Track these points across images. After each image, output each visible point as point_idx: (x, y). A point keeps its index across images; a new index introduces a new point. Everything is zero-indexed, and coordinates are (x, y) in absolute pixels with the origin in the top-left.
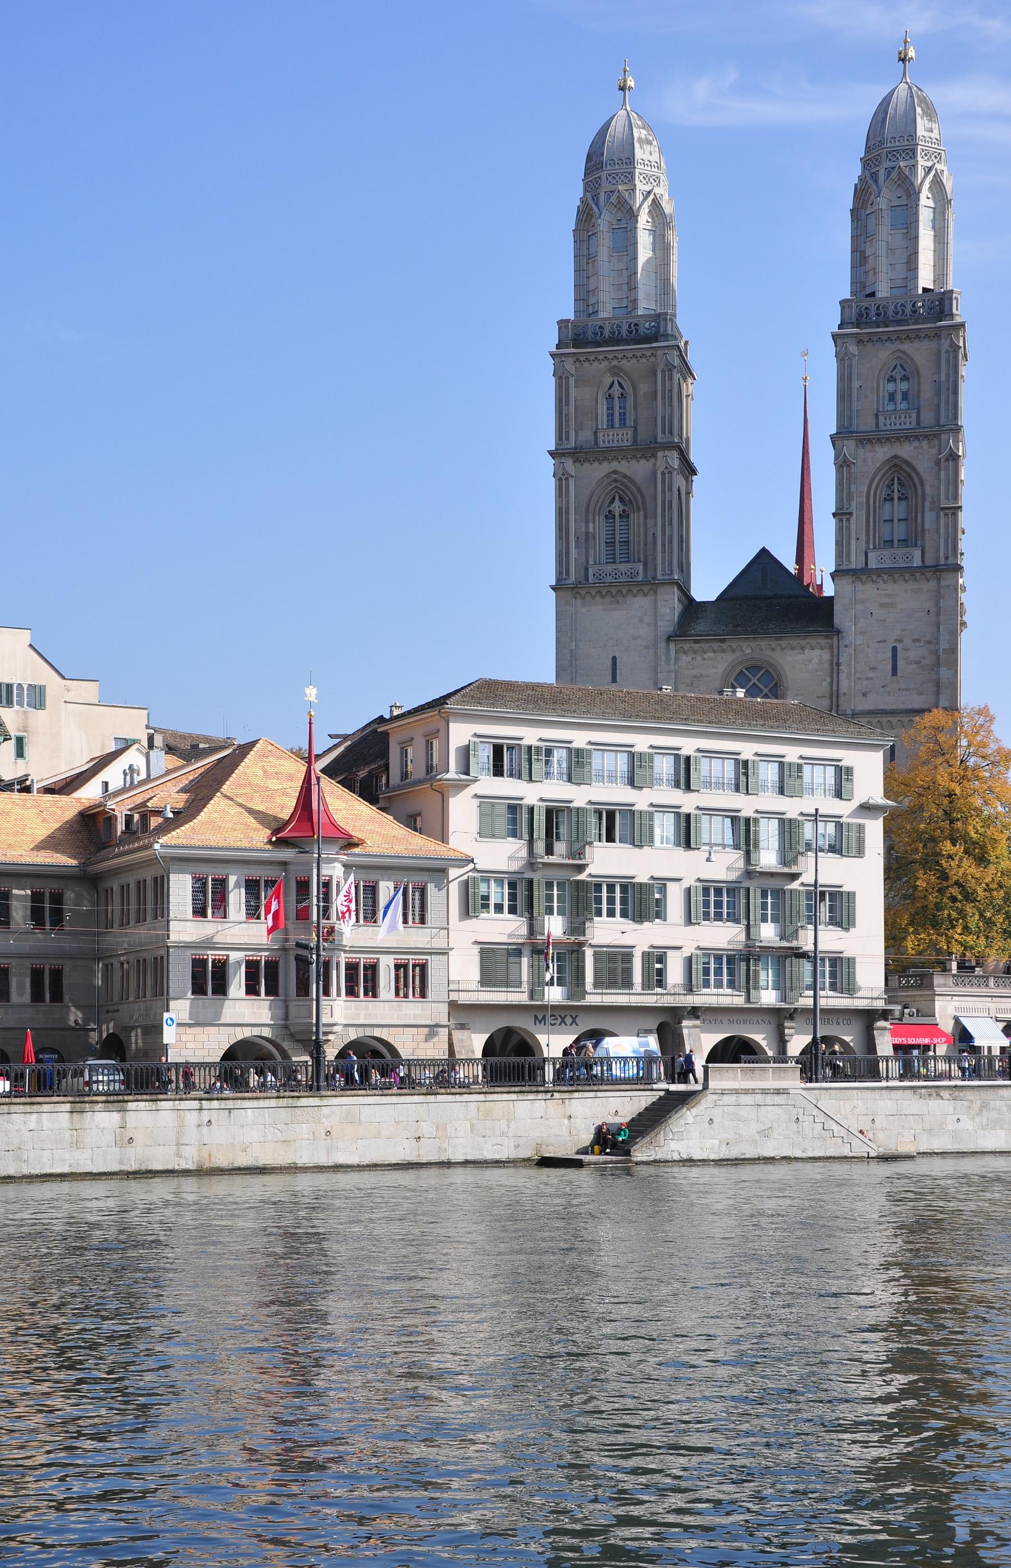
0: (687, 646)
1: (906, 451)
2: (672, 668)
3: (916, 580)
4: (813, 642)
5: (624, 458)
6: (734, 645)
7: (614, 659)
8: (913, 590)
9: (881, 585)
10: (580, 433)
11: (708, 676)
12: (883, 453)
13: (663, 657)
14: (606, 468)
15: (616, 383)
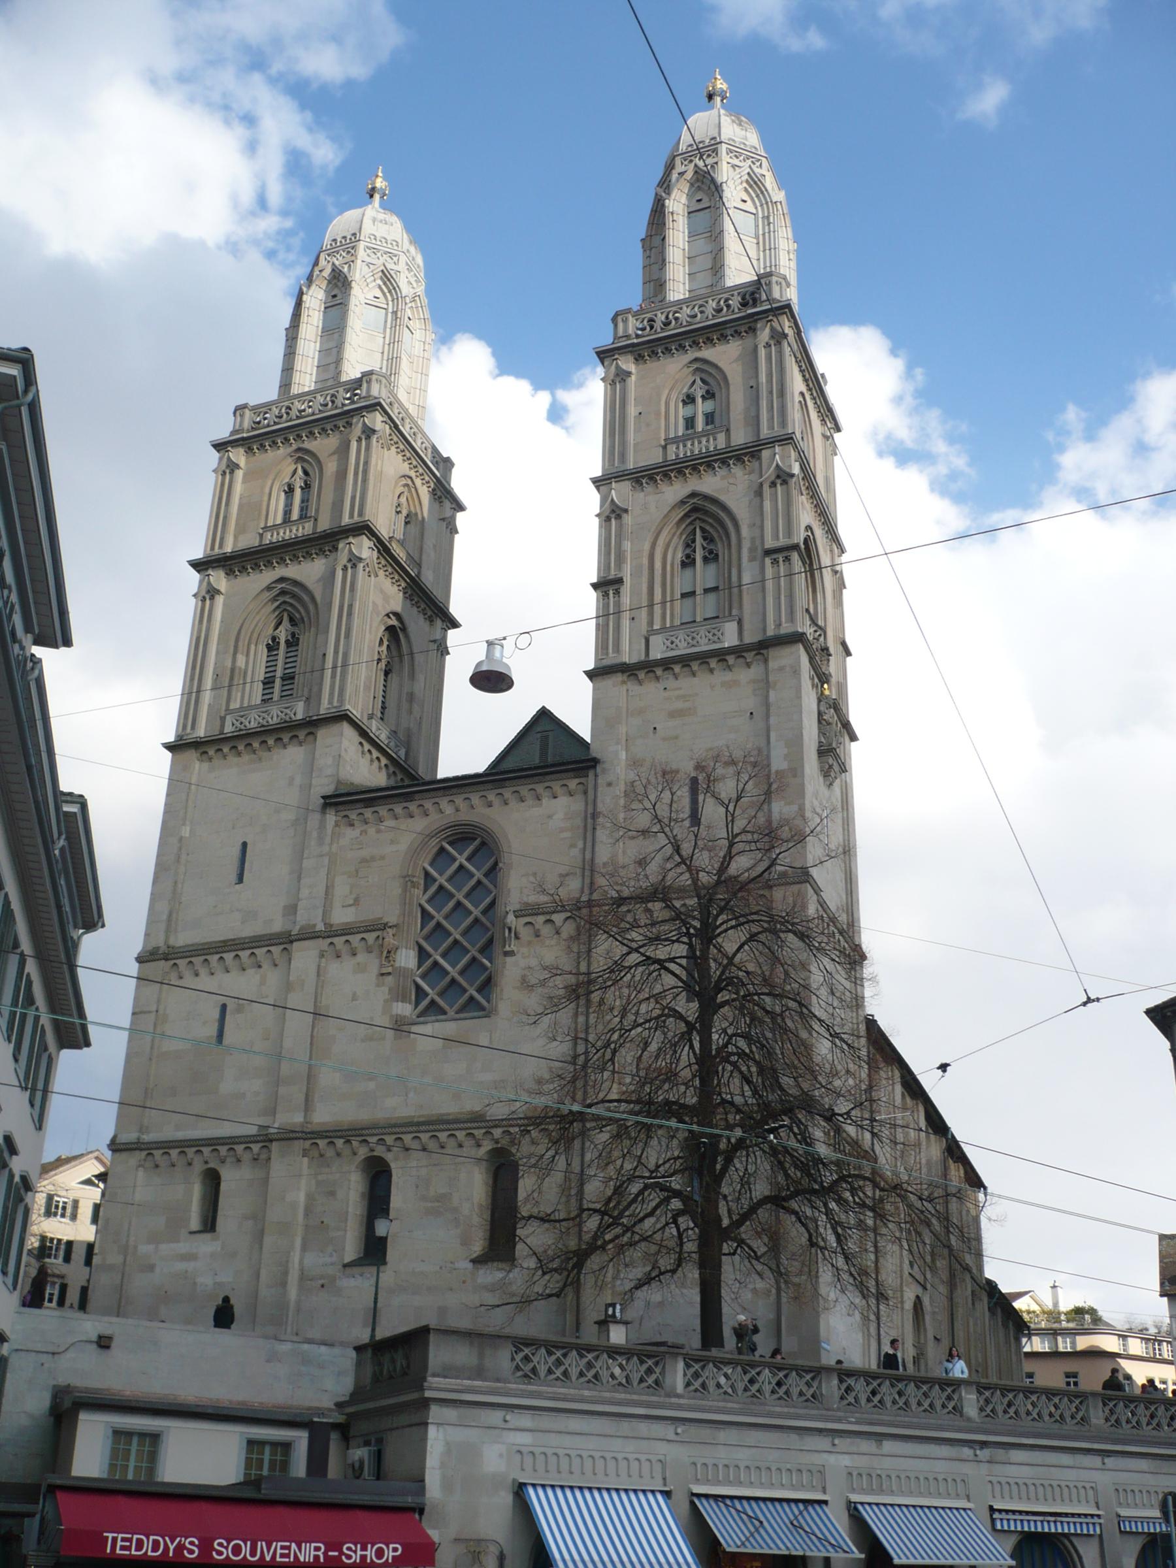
0: (353, 815)
1: (709, 483)
2: (326, 849)
3: (729, 668)
4: (556, 786)
5: (295, 558)
6: (428, 804)
7: (245, 845)
8: (723, 684)
9: (671, 683)
10: (241, 538)
11: (382, 858)
12: (674, 491)
13: (315, 834)
14: (268, 576)
15: (300, 472)
